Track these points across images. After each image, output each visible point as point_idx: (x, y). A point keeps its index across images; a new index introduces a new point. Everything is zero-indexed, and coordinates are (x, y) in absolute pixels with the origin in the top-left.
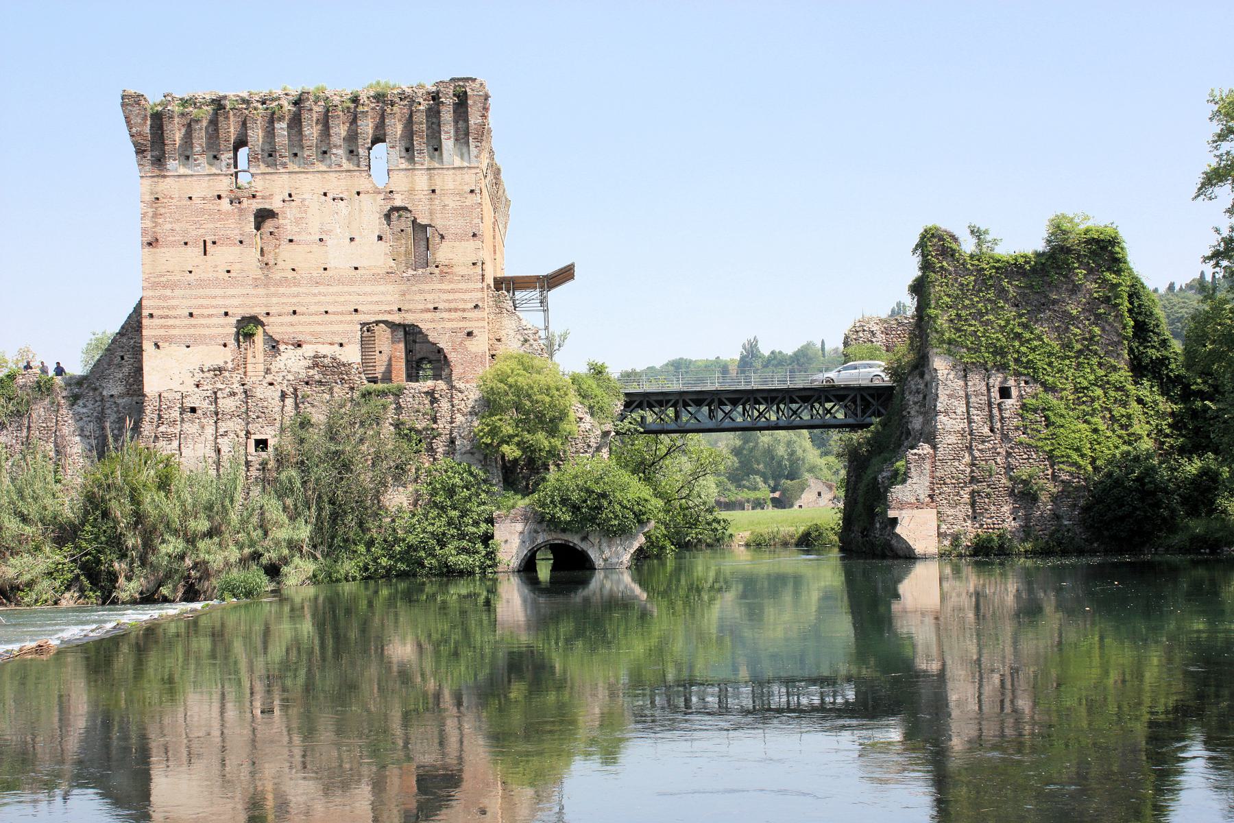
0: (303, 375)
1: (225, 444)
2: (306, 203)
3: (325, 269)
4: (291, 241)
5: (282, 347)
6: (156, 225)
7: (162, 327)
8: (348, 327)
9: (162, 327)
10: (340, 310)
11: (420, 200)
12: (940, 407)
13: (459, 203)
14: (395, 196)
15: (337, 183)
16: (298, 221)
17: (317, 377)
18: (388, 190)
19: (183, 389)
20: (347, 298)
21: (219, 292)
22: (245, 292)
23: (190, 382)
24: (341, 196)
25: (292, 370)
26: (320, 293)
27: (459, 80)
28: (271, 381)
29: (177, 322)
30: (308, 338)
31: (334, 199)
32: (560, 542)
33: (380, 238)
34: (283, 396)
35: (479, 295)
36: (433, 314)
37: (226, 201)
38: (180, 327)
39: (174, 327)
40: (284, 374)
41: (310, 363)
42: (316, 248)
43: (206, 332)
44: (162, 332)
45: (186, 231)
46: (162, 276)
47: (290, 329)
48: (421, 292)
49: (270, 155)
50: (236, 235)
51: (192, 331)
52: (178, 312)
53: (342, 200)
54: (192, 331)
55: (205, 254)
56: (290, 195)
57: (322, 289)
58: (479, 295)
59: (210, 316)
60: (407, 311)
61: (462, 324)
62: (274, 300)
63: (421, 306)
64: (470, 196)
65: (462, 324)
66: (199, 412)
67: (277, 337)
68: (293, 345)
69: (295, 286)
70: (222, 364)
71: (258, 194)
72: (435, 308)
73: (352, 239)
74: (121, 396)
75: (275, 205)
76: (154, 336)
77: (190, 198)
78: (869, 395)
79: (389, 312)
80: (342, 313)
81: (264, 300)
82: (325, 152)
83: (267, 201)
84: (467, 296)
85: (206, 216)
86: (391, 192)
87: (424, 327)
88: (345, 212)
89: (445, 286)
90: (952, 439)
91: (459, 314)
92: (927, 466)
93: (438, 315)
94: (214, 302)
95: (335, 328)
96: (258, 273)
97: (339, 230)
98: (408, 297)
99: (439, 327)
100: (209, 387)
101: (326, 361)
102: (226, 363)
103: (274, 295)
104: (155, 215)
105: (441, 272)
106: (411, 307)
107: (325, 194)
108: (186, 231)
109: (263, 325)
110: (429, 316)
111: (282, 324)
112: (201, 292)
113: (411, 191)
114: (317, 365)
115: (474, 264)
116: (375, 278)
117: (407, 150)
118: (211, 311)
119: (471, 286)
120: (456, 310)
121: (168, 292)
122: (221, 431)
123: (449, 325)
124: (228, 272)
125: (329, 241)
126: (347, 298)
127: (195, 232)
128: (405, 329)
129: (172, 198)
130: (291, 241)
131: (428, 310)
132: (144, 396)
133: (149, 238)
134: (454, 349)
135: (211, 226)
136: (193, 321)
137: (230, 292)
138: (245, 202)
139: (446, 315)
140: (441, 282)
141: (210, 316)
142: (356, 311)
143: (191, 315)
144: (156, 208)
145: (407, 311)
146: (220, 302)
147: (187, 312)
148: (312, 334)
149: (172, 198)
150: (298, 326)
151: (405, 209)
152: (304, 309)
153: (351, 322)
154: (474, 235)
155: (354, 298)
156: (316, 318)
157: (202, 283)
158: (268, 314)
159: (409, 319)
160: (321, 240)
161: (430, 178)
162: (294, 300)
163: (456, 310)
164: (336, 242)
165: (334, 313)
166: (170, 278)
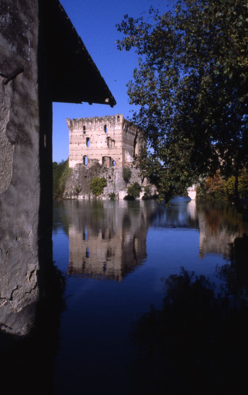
8: (100, 157)
9: (72, 157)
16: (93, 139)
21: (80, 151)
33: (106, 142)
37: (82, 136)
38: (74, 157)
39: (74, 157)
42: (95, 144)
43: (78, 158)
44: (72, 158)
48: (112, 151)
50: (83, 142)
55: (79, 145)
57: (96, 151)
62: (89, 153)
63: (112, 154)
65: (118, 157)
75: (89, 136)
79: (107, 155)
86: (108, 134)
89: (116, 150)
93: (114, 155)
95: (98, 157)
96: (86, 148)
99: (115, 157)
106: (110, 154)
108: (76, 141)
109: (87, 157)
110: (113, 155)
112: (79, 151)
116: (105, 149)
120: (117, 154)
121: (73, 151)
125: (98, 143)
131: (112, 154)
134: (117, 161)
136: (76, 156)
137: (82, 151)
138: (85, 136)
139: (116, 155)
141: (79, 155)
143: (76, 155)
147: (75, 155)
153: (101, 156)
157: (78, 150)
158: (88, 155)
159: (110, 156)
163: (117, 154)
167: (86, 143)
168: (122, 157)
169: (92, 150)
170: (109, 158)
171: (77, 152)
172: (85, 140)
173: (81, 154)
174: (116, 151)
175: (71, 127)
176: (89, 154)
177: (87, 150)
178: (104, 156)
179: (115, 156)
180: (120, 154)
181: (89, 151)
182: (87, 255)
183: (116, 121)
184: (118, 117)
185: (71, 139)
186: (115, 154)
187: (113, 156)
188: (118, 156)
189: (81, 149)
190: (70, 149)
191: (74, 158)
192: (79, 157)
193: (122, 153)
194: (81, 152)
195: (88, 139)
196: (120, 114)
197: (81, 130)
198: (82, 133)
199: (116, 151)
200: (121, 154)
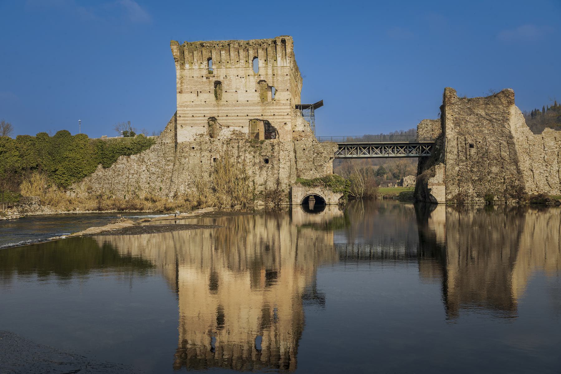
0: (229, 137)
2: (231, 79)
3: (237, 101)
4: (226, 92)
5: (223, 128)
6: (182, 86)
7: (183, 120)
9: (183, 120)
11: (269, 78)
12: (448, 151)
13: (283, 79)
14: (261, 76)
15: (241, 72)
16: (228, 85)
17: (234, 138)
18: (259, 74)
19: (190, 141)
23: (192, 140)
24: (243, 76)
25: (226, 135)
28: (219, 139)
29: (188, 119)
31: (241, 77)
32: (314, 194)
33: (256, 91)
34: (223, 143)
35: (289, 110)
36: (273, 116)
37: (205, 78)
39: (187, 120)
40: (224, 136)
42: (234, 94)
43: (198, 122)
44: (183, 122)
45: (191, 88)
47: (225, 121)
48: (269, 109)
49: (220, 62)
51: (193, 122)
52: (189, 115)
53: (243, 78)
54: (193, 122)
56: (226, 76)
57: (236, 108)
58: (289, 110)
59: (199, 117)
60: (264, 115)
62: (220, 112)
64: (286, 76)
66: (195, 149)
68: (226, 127)
70: (203, 133)
71: (215, 76)
72: (274, 115)
73: (246, 91)
75: (221, 79)
77: (193, 77)
79: (259, 116)
81: (217, 112)
82: (238, 61)
84: (284, 111)
86: (260, 75)
87: (270, 121)
88: (244, 82)
90: (452, 162)
91: (282, 117)
92: (442, 170)
93: (275, 117)
95: (240, 121)
96: (215, 102)
97: (242, 88)
99: (275, 121)
100: (199, 141)
101: (237, 132)
102: (204, 132)
105: (276, 103)
106: (266, 114)
107: (238, 76)
108: (191, 88)
112: (196, 108)
113: (267, 74)
114: (234, 133)
115: (287, 100)
116: (254, 104)
117: (265, 61)
118: (199, 115)
119: (286, 107)
120: (281, 115)
121: (185, 109)
122: (202, 155)
123: (279, 120)
124: (205, 102)
125: (239, 92)
127: (194, 89)
128: (264, 122)
130: (226, 92)
131: (271, 115)
132: (177, 143)
134: (280, 129)
135: (200, 86)
136: (193, 118)
138: (211, 79)
140: (276, 105)
141: (199, 117)
142: (247, 115)
144: (182, 80)
145: (264, 115)
146: (203, 112)
147: (191, 115)
148: (233, 123)
150: (229, 121)
152: (230, 115)
154: (288, 90)
155: (247, 111)
156: (235, 118)
157: (197, 106)
158: (218, 116)
159: (265, 118)
161: (273, 70)
162: (226, 112)
163: (281, 115)
164: (241, 91)
165: (240, 116)
166: (186, 104)
167: (213, 92)
169: (227, 106)
171: (193, 110)
172: (213, 87)
175: (182, 60)
176: (220, 115)
177: (214, 106)
178: (253, 118)
181: (220, 108)
182: (221, 319)
183: (279, 48)
184: (283, 42)
185: (182, 83)
186: (276, 114)
187: (273, 119)
190: (178, 103)
194: (204, 110)
195: (218, 84)
198: (205, 72)
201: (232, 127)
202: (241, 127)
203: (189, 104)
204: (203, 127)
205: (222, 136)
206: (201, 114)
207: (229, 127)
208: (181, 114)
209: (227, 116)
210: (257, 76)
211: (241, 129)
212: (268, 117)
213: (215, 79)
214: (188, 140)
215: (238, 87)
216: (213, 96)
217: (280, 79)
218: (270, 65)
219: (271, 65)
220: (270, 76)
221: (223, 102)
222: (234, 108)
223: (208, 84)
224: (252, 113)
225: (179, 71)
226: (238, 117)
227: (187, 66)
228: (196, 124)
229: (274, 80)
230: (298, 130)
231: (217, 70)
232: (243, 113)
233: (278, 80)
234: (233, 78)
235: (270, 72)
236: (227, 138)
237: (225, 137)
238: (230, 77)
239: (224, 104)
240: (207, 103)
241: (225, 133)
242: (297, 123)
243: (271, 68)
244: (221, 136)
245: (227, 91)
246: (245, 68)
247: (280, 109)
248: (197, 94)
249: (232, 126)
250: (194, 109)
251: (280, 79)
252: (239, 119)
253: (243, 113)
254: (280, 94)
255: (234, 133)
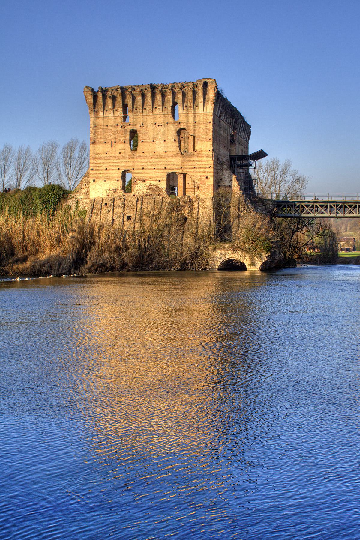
0: (145, 192)
1: (115, 217)
3: (155, 152)
5: (138, 182)
6: (95, 136)
7: (96, 174)
9: (96, 174)
10: (159, 168)
13: (205, 127)
14: (181, 124)
16: (145, 134)
17: (150, 193)
19: (103, 197)
20: (162, 163)
22: (126, 160)
23: (105, 194)
24: (161, 124)
26: (152, 161)
27: (206, 79)
29: (101, 172)
30: (148, 178)
31: (159, 126)
33: (175, 140)
34: (138, 200)
36: (194, 169)
39: (100, 174)
41: (147, 188)
42: (151, 144)
43: (112, 175)
45: (106, 138)
46: (96, 155)
47: (141, 175)
50: (123, 139)
52: (102, 168)
53: (161, 126)
55: (112, 146)
56: (143, 124)
57: (153, 160)
59: (113, 170)
60: (184, 168)
61: (204, 174)
62: (136, 164)
63: (190, 167)
64: (209, 124)
65: (204, 174)
67: (137, 178)
69: (143, 158)
70: (117, 188)
71: (131, 124)
72: (195, 167)
73: (165, 141)
74: (85, 199)
75: (138, 127)
76: (93, 177)
77: (107, 126)
78: (333, 205)
79: (177, 169)
80: (160, 169)
83: (135, 126)
84: (206, 163)
85: (113, 132)
88: (162, 130)
94: (115, 164)
96: (130, 153)
97: (160, 138)
98: (185, 163)
101: (154, 187)
102: (118, 187)
103: (137, 162)
104: (95, 132)
106: (185, 167)
107: (155, 124)
111: (138, 173)
112: (110, 161)
114: (150, 189)
115: (210, 150)
116: (173, 156)
119: (208, 159)
120: (202, 168)
121: (99, 161)
123: (200, 174)
124: (120, 153)
125: (157, 142)
126: (162, 163)
129: (101, 126)
130: (142, 141)
131: (192, 168)
133: (92, 141)
134: (201, 183)
135: (115, 136)
136: (107, 171)
137: (120, 161)
140: (198, 156)
141: (113, 170)
143: (106, 169)
145: (184, 168)
146: (117, 164)
148: (149, 177)
149: (101, 126)
150: (145, 174)
151: (185, 129)
153: (163, 172)
156: (151, 171)
158: (134, 169)
159: (185, 171)
160: (153, 141)
161: (195, 117)
162: (142, 164)
163: (202, 168)
165: (157, 169)
166: (100, 155)
168: (213, 173)
169: (144, 157)
170: (182, 174)
172: (128, 137)
173: (117, 168)
174: (198, 161)
176: (135, 168)
178: (171, 171)
179: (197, 172)
180: (208, 166)
181: (135, 160)
186: (197, 166)
187: (193, 172)
188: (205, 171)
189: (118, 154)
191: (101, 176)
192: (113, 174)
193: (212, 166)
194: (118, 163)
195: (134, 134)
196: (208, 79)
197: (119, 113)
198: (120, 120)
199: (198, 161)
200: (210, 167)
201: (148, 181)
202: (158, 181)
203: (102, 155)
204: (117, 182)
205: (137, 192)
206: (115, 166)
207: (145, 181)
208: (94, 166)
209: (143, 168)
210: (176, 124)
211: (158, 184)
212: (188, 170)
213: (131, 127)
214: (101, 196)
215: (155, 136)
216: (128, 147)
217: (202, 127)
218: (192, 112)
219: (192, 111)
220: (191, 124)
221: (139, 153)
222: (151, 160)
223: (124, 133)
224: (171, 165)
225: (93, 120)
226: (155, 170)
227: (101, 114)
228: (109, 178)
229: (196, 128)
230: (223, 184)
231: (134, 118)
232: (161, 165)
233: (199, 128)
234: (151, 127)
235: (191, 119)
236: (143, 193)
237: (141, 193)
238: (148, 125)
239: (141, 156)
240: (121, 154)
241: (140, 189)
242: (223, 177)
243: (192, 115)
244: (136, 191)
245: (144, 141)
246: (164, 114)
247: (202, 161)
248: (111, 144)
249: (148, 180)
250: (108, 161)
251: (202, 127)
252: (156, 172)
253: (161, 165)
254: (202, 144)
255: (150, 187)
